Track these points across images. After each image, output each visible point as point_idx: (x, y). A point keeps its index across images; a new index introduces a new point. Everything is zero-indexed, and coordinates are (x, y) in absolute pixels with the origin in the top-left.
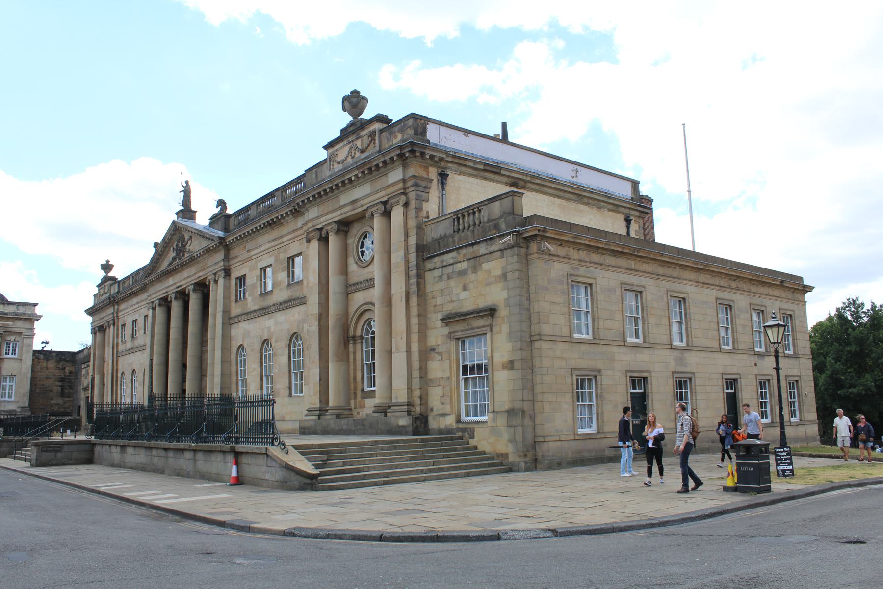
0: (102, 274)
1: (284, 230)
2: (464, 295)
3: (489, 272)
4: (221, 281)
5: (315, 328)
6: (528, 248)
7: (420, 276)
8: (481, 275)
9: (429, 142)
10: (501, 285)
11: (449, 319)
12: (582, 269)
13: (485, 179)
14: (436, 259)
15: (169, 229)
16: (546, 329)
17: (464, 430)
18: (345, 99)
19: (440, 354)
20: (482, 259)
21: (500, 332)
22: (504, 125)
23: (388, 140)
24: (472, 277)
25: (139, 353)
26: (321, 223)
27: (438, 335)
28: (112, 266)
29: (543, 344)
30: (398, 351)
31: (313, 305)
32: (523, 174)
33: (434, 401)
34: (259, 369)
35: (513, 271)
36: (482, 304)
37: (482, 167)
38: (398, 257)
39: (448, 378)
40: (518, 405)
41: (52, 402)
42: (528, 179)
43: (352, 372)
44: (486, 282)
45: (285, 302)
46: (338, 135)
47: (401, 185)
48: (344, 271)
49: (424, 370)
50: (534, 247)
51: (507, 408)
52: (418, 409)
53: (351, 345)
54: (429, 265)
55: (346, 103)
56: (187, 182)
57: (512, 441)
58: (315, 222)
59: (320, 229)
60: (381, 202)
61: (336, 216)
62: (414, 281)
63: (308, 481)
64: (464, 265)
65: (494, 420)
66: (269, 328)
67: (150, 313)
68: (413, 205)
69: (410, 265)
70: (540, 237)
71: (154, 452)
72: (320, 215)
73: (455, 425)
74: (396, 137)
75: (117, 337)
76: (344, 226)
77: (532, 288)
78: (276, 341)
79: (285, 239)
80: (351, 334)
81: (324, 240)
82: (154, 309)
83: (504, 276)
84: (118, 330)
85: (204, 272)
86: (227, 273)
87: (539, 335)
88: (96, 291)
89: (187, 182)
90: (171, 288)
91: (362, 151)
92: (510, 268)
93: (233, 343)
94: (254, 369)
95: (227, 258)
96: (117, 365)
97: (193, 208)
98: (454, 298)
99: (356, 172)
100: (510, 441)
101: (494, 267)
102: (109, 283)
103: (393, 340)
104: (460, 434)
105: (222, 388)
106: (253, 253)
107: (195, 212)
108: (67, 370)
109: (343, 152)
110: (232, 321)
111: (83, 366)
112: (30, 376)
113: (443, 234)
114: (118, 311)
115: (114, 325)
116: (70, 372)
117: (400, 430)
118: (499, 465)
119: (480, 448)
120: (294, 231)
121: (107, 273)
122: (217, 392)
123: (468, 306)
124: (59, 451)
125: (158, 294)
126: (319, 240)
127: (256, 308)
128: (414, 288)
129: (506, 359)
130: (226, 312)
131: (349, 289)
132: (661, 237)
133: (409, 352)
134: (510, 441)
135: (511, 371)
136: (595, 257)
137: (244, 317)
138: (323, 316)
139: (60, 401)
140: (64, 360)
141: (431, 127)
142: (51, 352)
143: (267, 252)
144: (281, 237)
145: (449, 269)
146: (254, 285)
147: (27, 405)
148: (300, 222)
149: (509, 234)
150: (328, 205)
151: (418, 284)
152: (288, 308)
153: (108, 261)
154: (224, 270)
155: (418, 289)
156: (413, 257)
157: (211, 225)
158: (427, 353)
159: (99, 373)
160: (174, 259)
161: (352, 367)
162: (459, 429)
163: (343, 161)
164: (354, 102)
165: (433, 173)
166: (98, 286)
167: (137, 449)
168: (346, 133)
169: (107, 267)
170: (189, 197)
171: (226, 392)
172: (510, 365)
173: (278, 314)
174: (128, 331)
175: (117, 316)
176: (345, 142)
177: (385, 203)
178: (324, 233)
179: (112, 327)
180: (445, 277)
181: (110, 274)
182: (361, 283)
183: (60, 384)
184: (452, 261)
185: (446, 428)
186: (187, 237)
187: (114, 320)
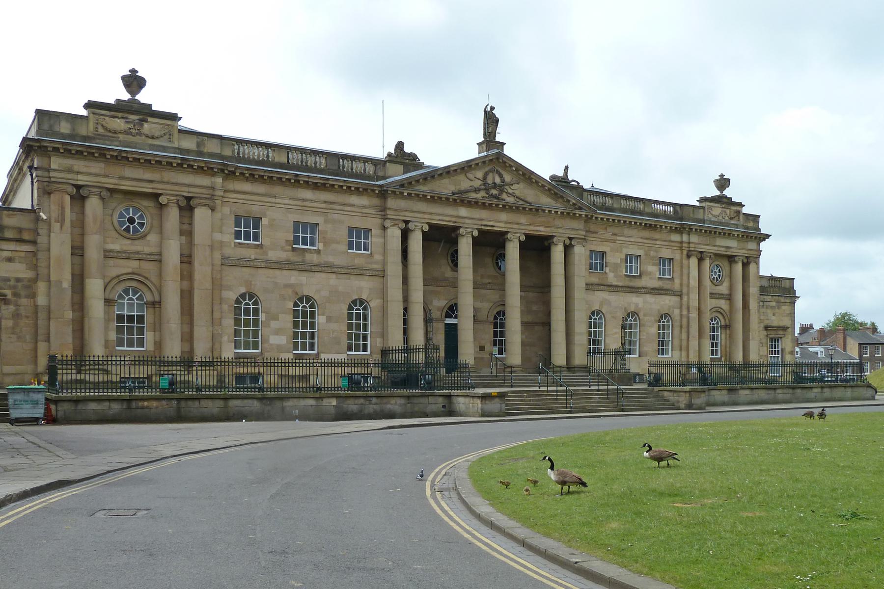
1: (657, 235)
2: (774, 318)
24: (777, 310)
25: (334, 276)
26: (703, 248)
36: (781, 324)
59: (701, 253)
61: (714, 249)
64: (774, 304)
66: (637, 305)
78: (644, 315)
79: (658, 242)
85: (548, 229)
90: (467, 221)
91: (731, 219)
94: (616, 333)
106: (618, 238)
109: (717, 210)
123: (775, 324)
125: (427, 216)
127: (620, 284)
137: (602, 287)
143: (637, 244)
144: (656, 240)
146: (616, 267)
148: (675, 237)
152: (659, 294)
160: (477, 190)
164: (723, 183)
166: (89, 105)
173: (648, 296)
174: (276, 235)
176: (719, 205)
186: (508, 178)
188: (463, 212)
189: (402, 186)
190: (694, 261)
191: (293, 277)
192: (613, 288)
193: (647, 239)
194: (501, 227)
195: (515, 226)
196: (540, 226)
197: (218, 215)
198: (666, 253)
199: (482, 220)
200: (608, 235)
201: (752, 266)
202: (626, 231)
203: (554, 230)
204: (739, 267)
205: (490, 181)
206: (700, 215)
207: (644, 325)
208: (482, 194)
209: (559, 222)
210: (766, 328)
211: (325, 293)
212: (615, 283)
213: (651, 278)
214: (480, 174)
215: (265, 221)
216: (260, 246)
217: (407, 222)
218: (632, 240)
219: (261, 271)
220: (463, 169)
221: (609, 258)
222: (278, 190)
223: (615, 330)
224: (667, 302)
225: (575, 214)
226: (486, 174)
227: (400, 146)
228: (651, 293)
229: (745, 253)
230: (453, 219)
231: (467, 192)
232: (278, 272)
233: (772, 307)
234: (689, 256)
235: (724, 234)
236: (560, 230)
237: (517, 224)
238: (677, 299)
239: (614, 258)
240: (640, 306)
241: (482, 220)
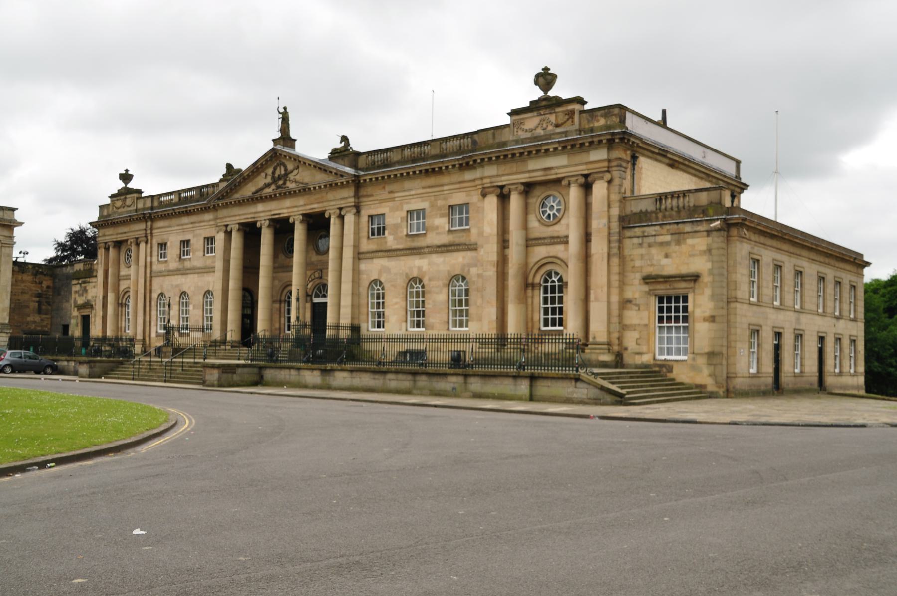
0: (121, 185)
1: (445, 179)
2: (665, 261)
3: (693, 246)
4: (350, 219)
5: (491, 273)
6: (728, 231)
7: (620, 241)
8: (684, 248)
9: (627, 128)
10: (705, 257)
11: (648, 279)
12: (756, 248)
13: (656, 160)
14: (637, 229)
15: (265, 155)
16: (739, 294)
17: (661, 366)
18: (538, 76)
19: (638, 305)
20: (686, 235)
21: (703, 293)
22: (664, 112)
23: (588, 121)
24: (674, 248)
25: (196, 275)
26: (503, 181)
27: (636, 290)
28: (131, 176)
29: (738, 305)
30: (597, 300)
31: (490, 251)
32: (680, 157)
33: (630, 340)
34: (404, 304)
35: (718, 248)
36: (684, 270)
37: (657, 151)
38: (598, 224)
39: (646, 325)
40: (717, 349)
41: (29, 319)
42: (681, 160)
43: (530, 313)
44: (692, 254)
45: (444, 246)
46: (528, 105)
47: (606, 164)
48: (525, 226)
49: (621, 316)
50: (734, 231)
51: (707, 350)
52: (616, 348)
53: (529, 291)
54: (628, 233)
55: (541, 80)
56: (285, 108)
57: (712, 375)
58: (493, 180)
59: (502, 187)
60: (582, 175)
61: (524, 178)
62: (615, 245)
63: (619, 399)
64: (668, 238)
65: (694, 359)
66: (420, 268)
67: (220, 237)
68: (617, 182)
69: (612, 231)
70: (740, 225)
71: (390, 376)
72: (512, 176)
73: (652, 362)
74: (598, 121)
75: (151, 256)
76: (528, 188)
77: (731, 262)
78: (430, 280)
79: (445, 188)
80: (530, 280)
81: (504, 198)
82: (228, 234)
83: (709, 251)
84: (152, 247)
85: (321, 205)
86: (358, 209)
87: (735, 298)
88: (108, 201)
89: (285, 108)
90: (262, 215)
91: (557, 126)
92: (715, 245)
93: (364, 277)
94: (396, 304)
95: (357, 195)
96: (151, 285)
97: (292, 135)
98: (655, 262)
99: (556, 145)
100: (710, 375)
101: (700, 243)
102: (135, 195)
103: (592, 292)
104: (657, 369)
105: (353, 318)
106: (396, 195)
107: (295, 140)
108: (45, 284)
109: (532, 121)
110: (361, 256)
111: (74, 282)
112: (9, 289)
113: (644, 210)
114: (152, 229)
115: (146, 242)
116: (48, 287)
117: (604, 365)
118: (698, 393)
119: (678, 380)
120: (460, 183)
121: (126, 184)
122: (346, 321)
124: (234, 373)
125: (237, 218)
126: (498, 196)
127: (400, 246)
128: (615, 250)
129: (707, 314)
130: (356, 246)
131: (530, 242)
132: (742, 206)
133: (609, 303)
134: (710, 375)
135: (712, 324)
136: (762, 239)
137: (380, 254)
138: (503, 261)
139: (37, 318)
140: (42, 273)
141: (628, 115)
142: (25, 264)
144: (442, 185)
145: (651, 240)
146: (396, 227)
147: (7, 322)
148: (469, 175)
149: (717, 220)
150: (512, 167)
151: (619, 248)
152: (448, 251)
153: (127, 171)
154: (355, 206)
155: (617, 253)
156: (615, 226)
157: (330, 159)
158: (625, 303)
159: (113, 291)
160: (267, 186)
161: (530, 309)
162: (656, 365)
163: (531, 130)
164: (545, 79)
165: (627, 156)
166: (112, 197)
167: (355, 374)
168: (535, 106)
169: (126, 177)
170: (288, 124)
171: (356, 322)
172: (712, 319)
174: (173, 251)
175: (152, 233)
176: (535, 113)
177: (586, 176)
178: (505, 191)
179: (142, 245)
180: (645, 245)
181: (130, 186)
182: (544, 238)
183: (37, 299)
184: (654, 233)
185: (642, 364)
186: (290, 167)
187: (146, 237)
188: (260, 207)
189: (219, 199)
190: (492, 202)
191: (178, 280)
192: (390, 253)
193: (429, 187)
194: (284, 213)
195: (295, 209)
196: (312, 204)
197: (149, 245)
198: (458, 198)
199: (270, 211)
200: (384, 194)
201: (599, 190)
202: (407, 184)
203: (325, 204)
204: (574, 194)
205: (277, 173)
206: (507, 136)
207: (429, 292)
208: (273, 187)
209: (331, 195)
210: (648, 279)
211: (192, 288)
212: (394, 247)
213: (437, 234)
214: (270, 171)
215: (169, 244)
216: (166, 261)
217: (226, 226)
218: (413, 193)
219: (167, 278)
220: (252, 172)
221: (390, 221)
222: (175, 221)
223: (395, 301)
224: (457, 261)
225: (336, 184)
226: (275, 169)
227: (229, 167)
228: (437, 252)
229: (583, 169)
230: (252, 216)
231: (261, 189)
232: (173, 277)
233: (662, 244)
234: (484, 195)
235: (530, 153)
236: (330, 203)
237: (296, 207)
238: (469, 254)
239: (394, 218)
240: (425, 268)
241: (270, 211)
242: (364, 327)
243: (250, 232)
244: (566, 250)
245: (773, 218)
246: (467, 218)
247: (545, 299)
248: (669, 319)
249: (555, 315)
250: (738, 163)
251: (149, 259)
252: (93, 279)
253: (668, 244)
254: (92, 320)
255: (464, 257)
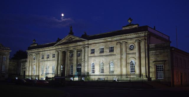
22: (155, 27)
108: (15, 64)
111: (22, 63)
116: (16, 65)
183: (13, 67)
234: (117, 44)
242: (90, 73)
243: (64, 53)
244: (136, 56)
245: (176, 48)
246: (113, 49)
247: (131, 66)
248: (159, 71)
249: (133, 70)
250: (169, 37)
251: (39, 58)
252: (26, 63)
253: (158, 54)
254: (26, 72)
255: (113, 58)
